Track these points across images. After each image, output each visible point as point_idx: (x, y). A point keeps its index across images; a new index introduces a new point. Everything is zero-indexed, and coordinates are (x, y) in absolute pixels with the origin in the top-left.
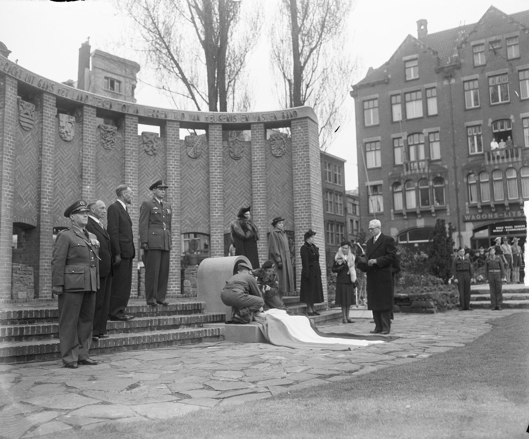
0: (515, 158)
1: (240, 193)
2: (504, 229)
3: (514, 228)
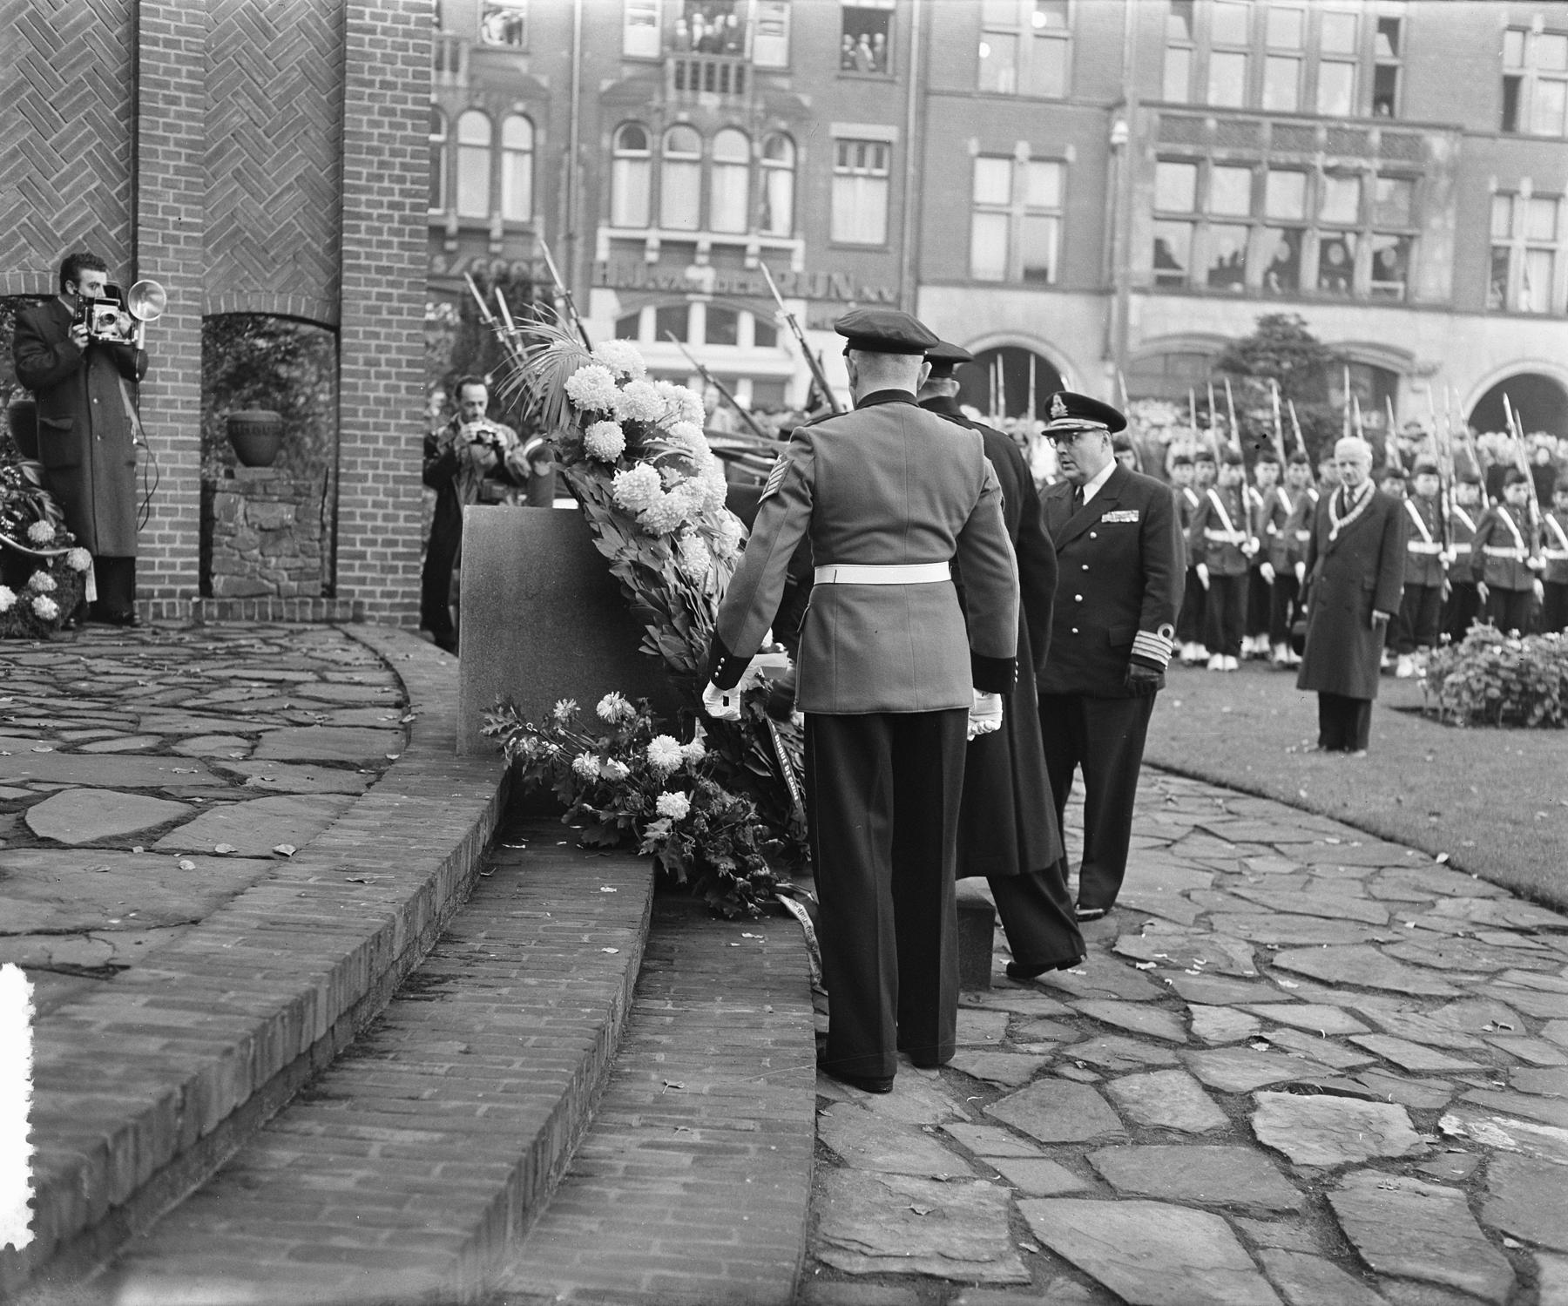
0: (447, 74)
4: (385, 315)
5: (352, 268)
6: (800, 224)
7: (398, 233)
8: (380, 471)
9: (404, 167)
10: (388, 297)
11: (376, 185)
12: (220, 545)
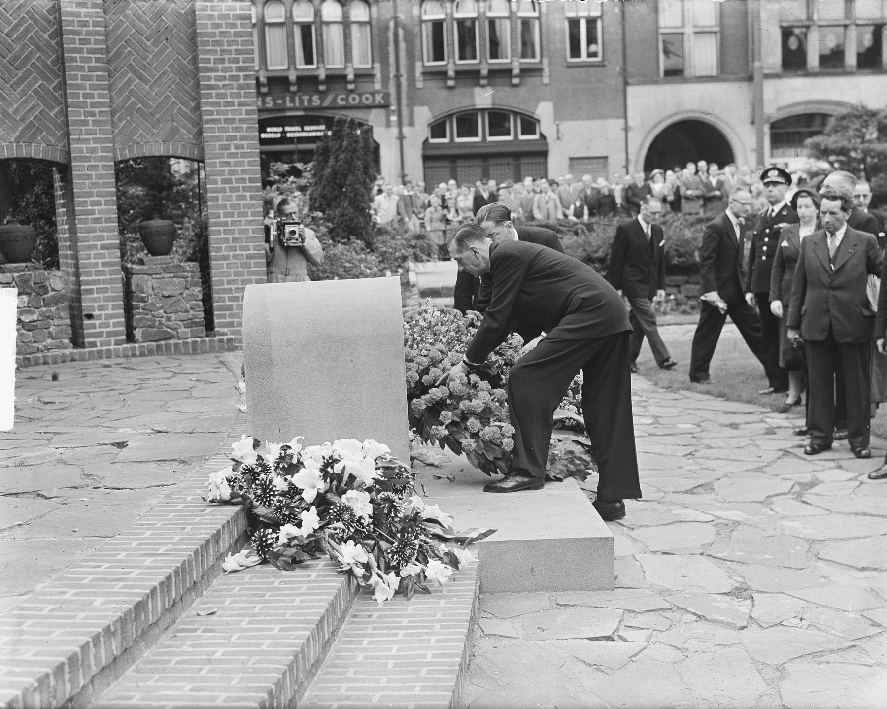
1: (18, 25)
2: (284, 132)
3: (303, 131)
4: (233, 150)
5: (208, 121)
6: (545, 53)
7: (238, 95)
8: (238, 252)
9: (238, 52)
10: (234, 138)
11: (220, 66)
12: (138, 308)
